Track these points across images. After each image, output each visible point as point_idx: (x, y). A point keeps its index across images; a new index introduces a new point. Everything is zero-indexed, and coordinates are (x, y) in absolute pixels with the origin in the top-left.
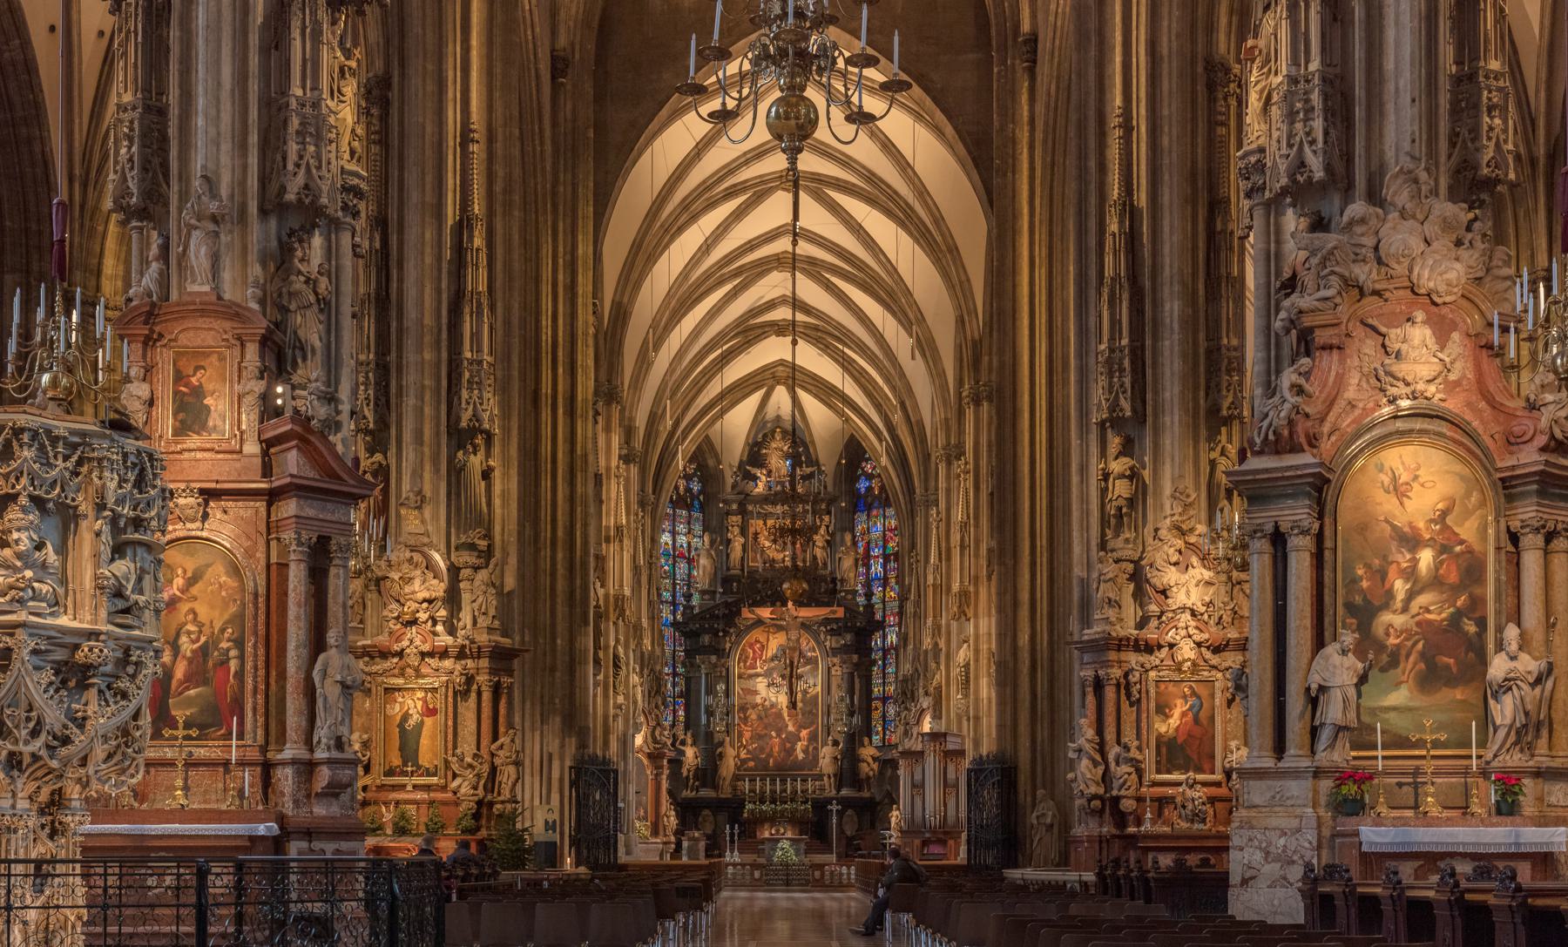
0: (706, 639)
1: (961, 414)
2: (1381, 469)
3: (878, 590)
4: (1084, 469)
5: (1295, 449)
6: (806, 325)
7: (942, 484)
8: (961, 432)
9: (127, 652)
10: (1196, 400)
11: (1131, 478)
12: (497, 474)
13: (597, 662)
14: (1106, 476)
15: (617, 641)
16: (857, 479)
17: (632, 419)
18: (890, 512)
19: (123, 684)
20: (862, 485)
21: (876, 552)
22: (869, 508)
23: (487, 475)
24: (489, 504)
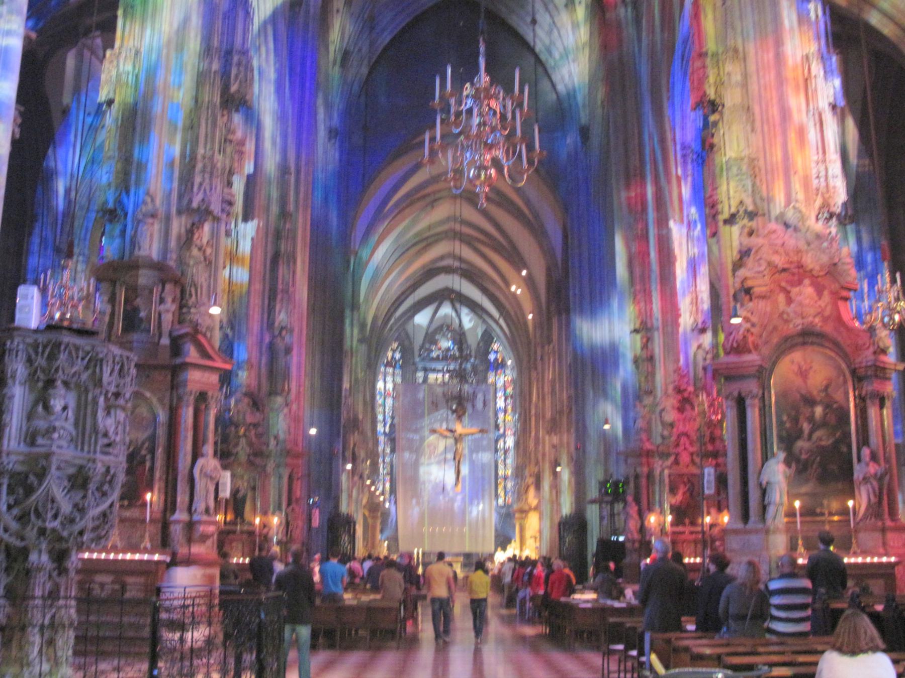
1: (549, 319)
2: (793, 362)
3: (501, 416)
15: (355, 445)
16: (490, 353)
19: (106, 487)
20: (492, 357)
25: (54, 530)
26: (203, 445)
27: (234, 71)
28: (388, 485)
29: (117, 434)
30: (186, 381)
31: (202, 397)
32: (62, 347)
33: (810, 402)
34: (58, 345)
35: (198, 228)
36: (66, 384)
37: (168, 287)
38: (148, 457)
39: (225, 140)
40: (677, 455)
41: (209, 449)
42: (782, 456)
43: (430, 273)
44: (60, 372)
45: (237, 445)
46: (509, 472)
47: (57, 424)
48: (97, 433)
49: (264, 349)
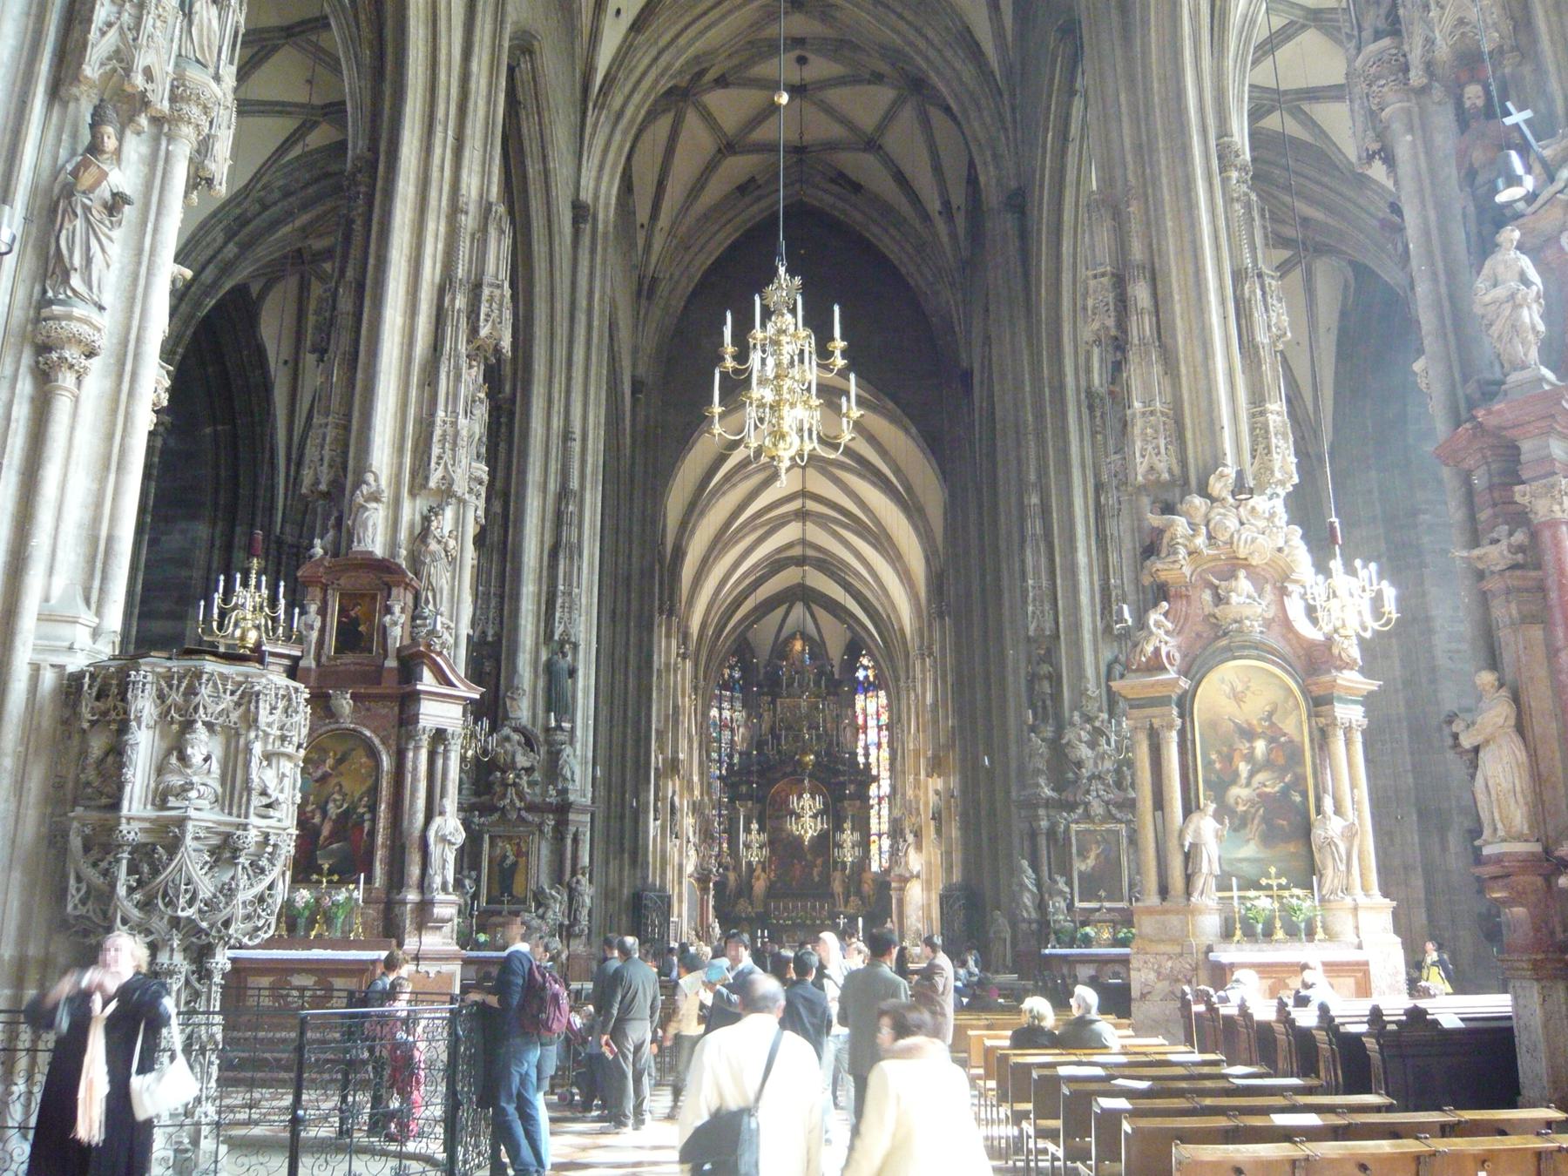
0: (744, 789)
2: (1223, 681)
3: (873, 751)
4: (1016, 671)
5: (1163, 669)
6: (818, 560)
7: (919, 675)
8: (931, 637)
9: (267, 836)
10: (1094, 622)
11: (1049, 677)
12: (581, 673)
13: (656, 810)
14: (1033, 679)
16: (856, 670)
17: (687, 627)
18: (882, 693)
19: (264, 862)
20: (861, 674)
21: (872, 723)
22: (866, 691)
23: (572, 673)
24: (574, 697)
25: (188, 918)
26: (442, 797)
27: (484, 309)
28: (725, 845)
29: (282, 791)
30: (417, 715)
31: (440, 736)
32: (205, 677)
33: (1249, 734)
34: (198, 675)
35: (436, 515)
36: (209, 726)
37: (394, 591)
38: (367, 816)
39: (474, 401)
40: (1087, 804)
41: (451, 803)
42: (1212, 807)
43: (776, 564)
44: (201, 710)
45: (504, 796)
46: (885, 827)
47: (195, 779)
48: (249, 790)
49: (541, 669)
